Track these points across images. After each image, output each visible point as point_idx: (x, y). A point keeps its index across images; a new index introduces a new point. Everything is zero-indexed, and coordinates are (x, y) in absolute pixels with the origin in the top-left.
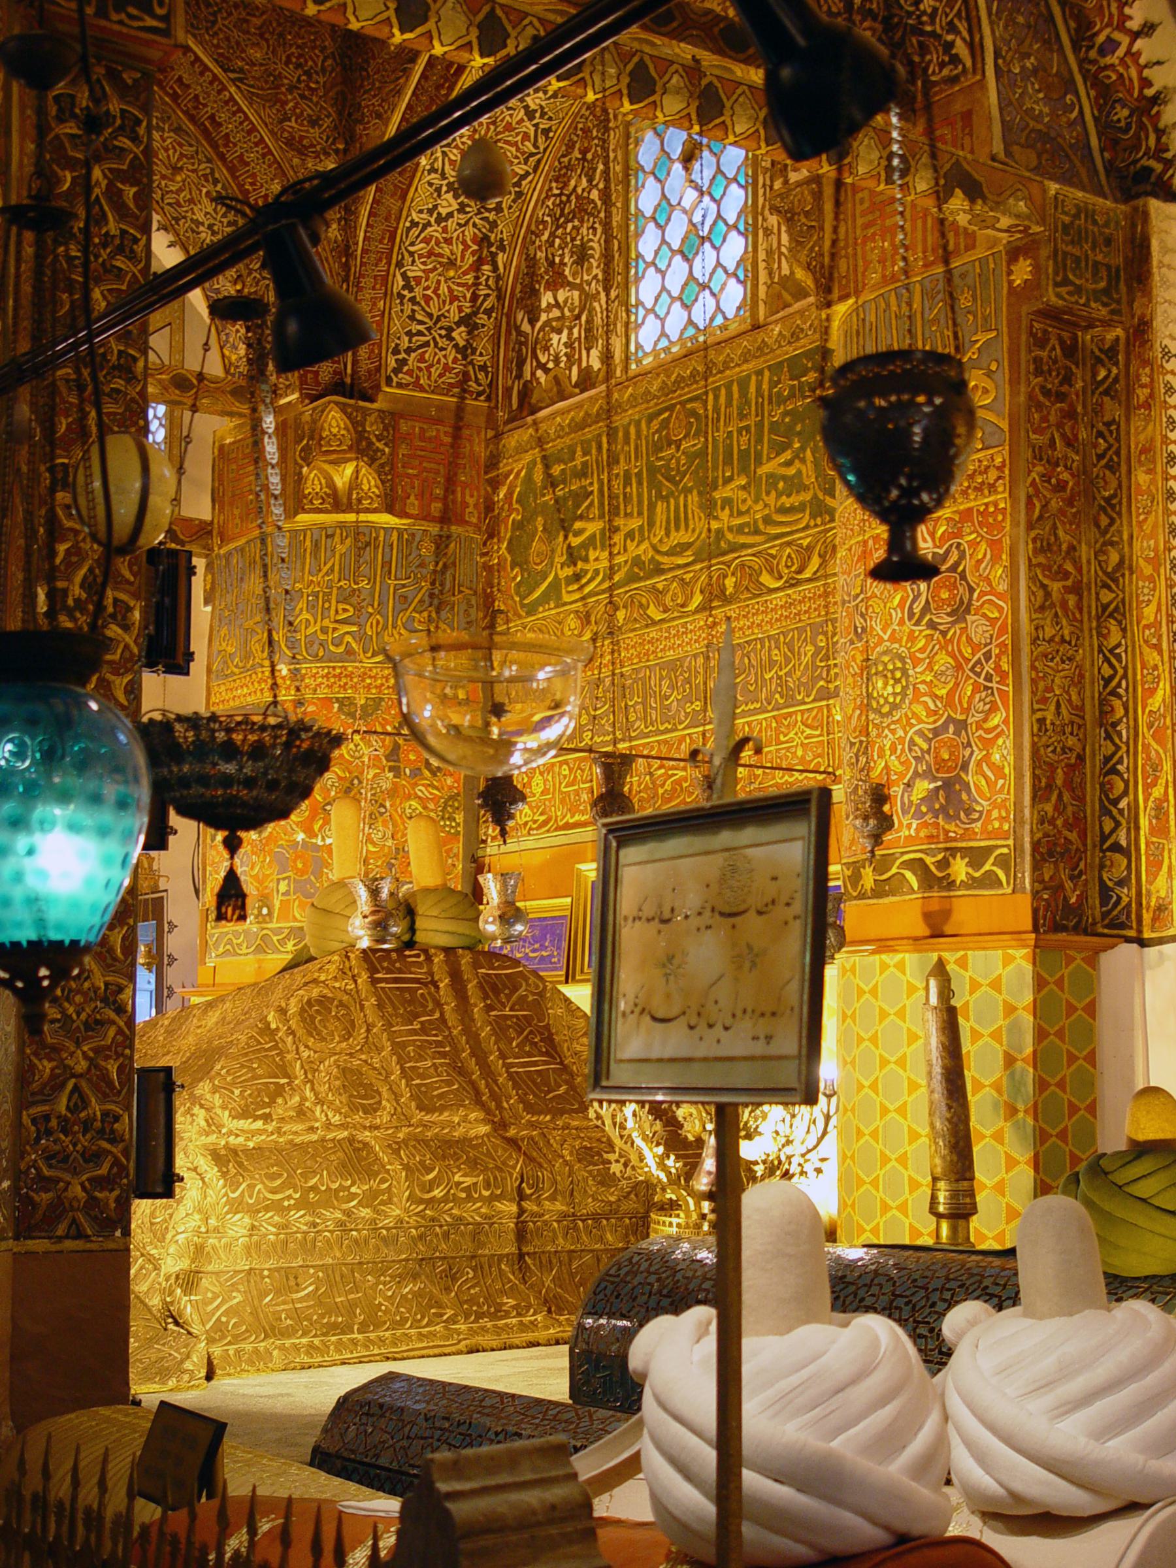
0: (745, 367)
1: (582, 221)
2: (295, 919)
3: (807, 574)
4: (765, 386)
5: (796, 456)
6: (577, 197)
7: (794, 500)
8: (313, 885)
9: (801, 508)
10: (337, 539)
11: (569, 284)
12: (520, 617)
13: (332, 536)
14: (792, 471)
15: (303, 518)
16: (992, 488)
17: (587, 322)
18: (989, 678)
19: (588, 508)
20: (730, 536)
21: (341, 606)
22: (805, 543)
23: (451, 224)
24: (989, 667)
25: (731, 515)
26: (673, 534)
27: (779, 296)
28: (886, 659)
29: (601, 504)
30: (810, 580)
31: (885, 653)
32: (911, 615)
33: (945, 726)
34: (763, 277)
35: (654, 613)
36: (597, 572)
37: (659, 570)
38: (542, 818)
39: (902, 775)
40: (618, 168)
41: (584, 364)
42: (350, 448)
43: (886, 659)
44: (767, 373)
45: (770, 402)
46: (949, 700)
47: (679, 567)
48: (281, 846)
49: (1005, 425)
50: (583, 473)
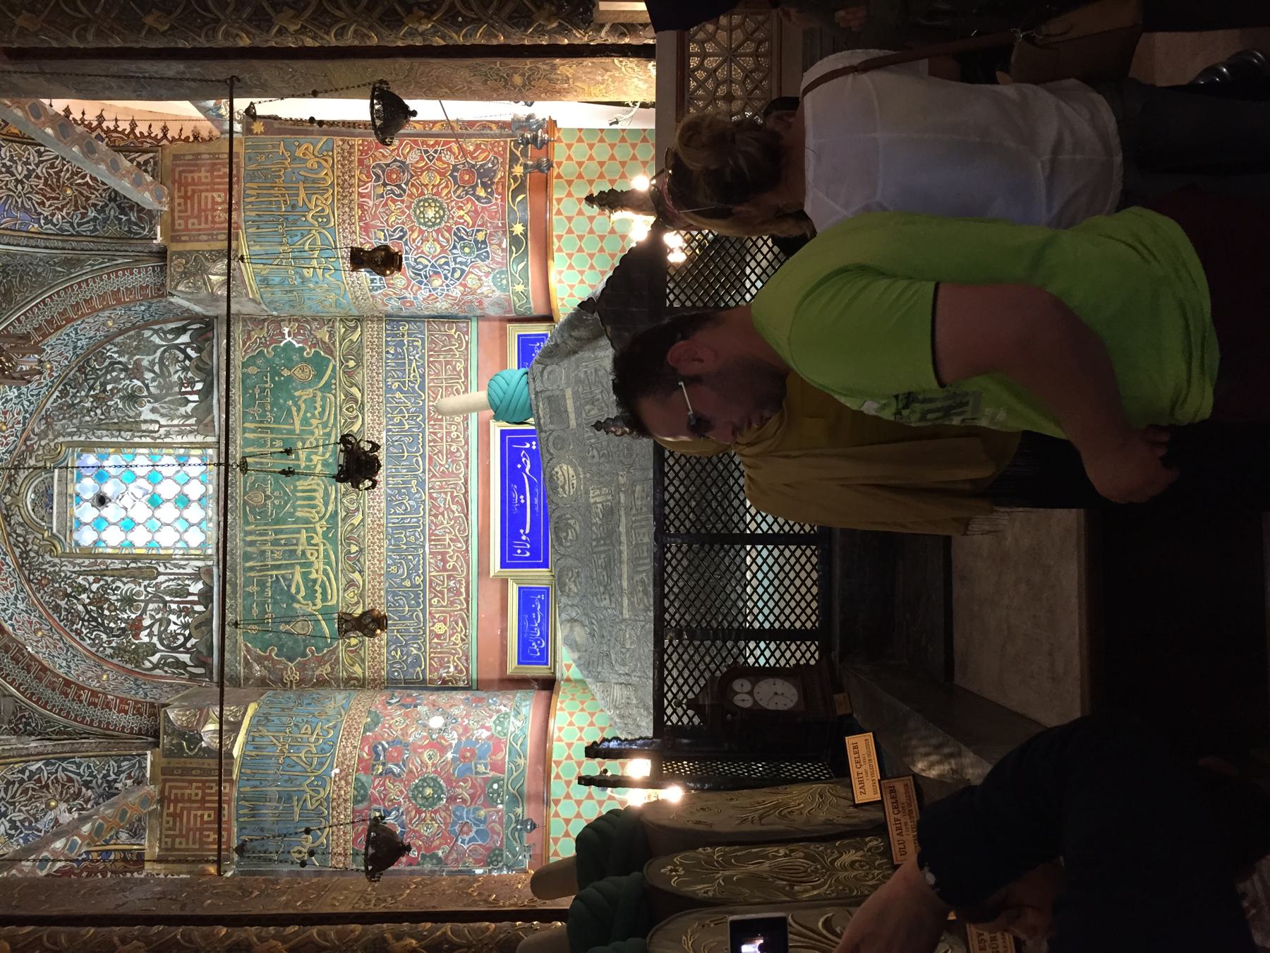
0: (238, 442)
1: (108, 600)
2: (504, 758)
3: (359, 395)
4: (252, 426)
5: (295, 404)
6: (90, 604)
7: (318, 405)
8: (482, 745)
9: (324, 399)
10: (256, 734)
11: (141, 615)
12: (338, 647)
13: (254, 737)
14: (303, 406)
15: (236, 752)
16: (352, 146)
17: (170, 595)
18: (436, 152)
19: (285, 579)
20: (328, 455)
21: (303, 731)
22: (343, 397)
23: (73, 666)
24: (431, 151)
25: (316, 453)
26: (316, 502)
27: (206, 425)
28: (418, 212)
29: (287, 566)
30: (363, 395)
31: (415, 212)
32: (400, 195)
33: (454, 178)
34: (191, 438)
35: (356, 521)
36: (325, 570)
37: (335, 514)
38: (460, 624)
39: (473, 203)
40: (87, 562)
41: (196, 598)
42: (201, 710)
43: (418, 212)
44: (246, 425)
45: (262, 422)
46: (442, 175)
47: (336, 498)
48: (454, 770)
49: (325, 138)
50: (262, 584)
